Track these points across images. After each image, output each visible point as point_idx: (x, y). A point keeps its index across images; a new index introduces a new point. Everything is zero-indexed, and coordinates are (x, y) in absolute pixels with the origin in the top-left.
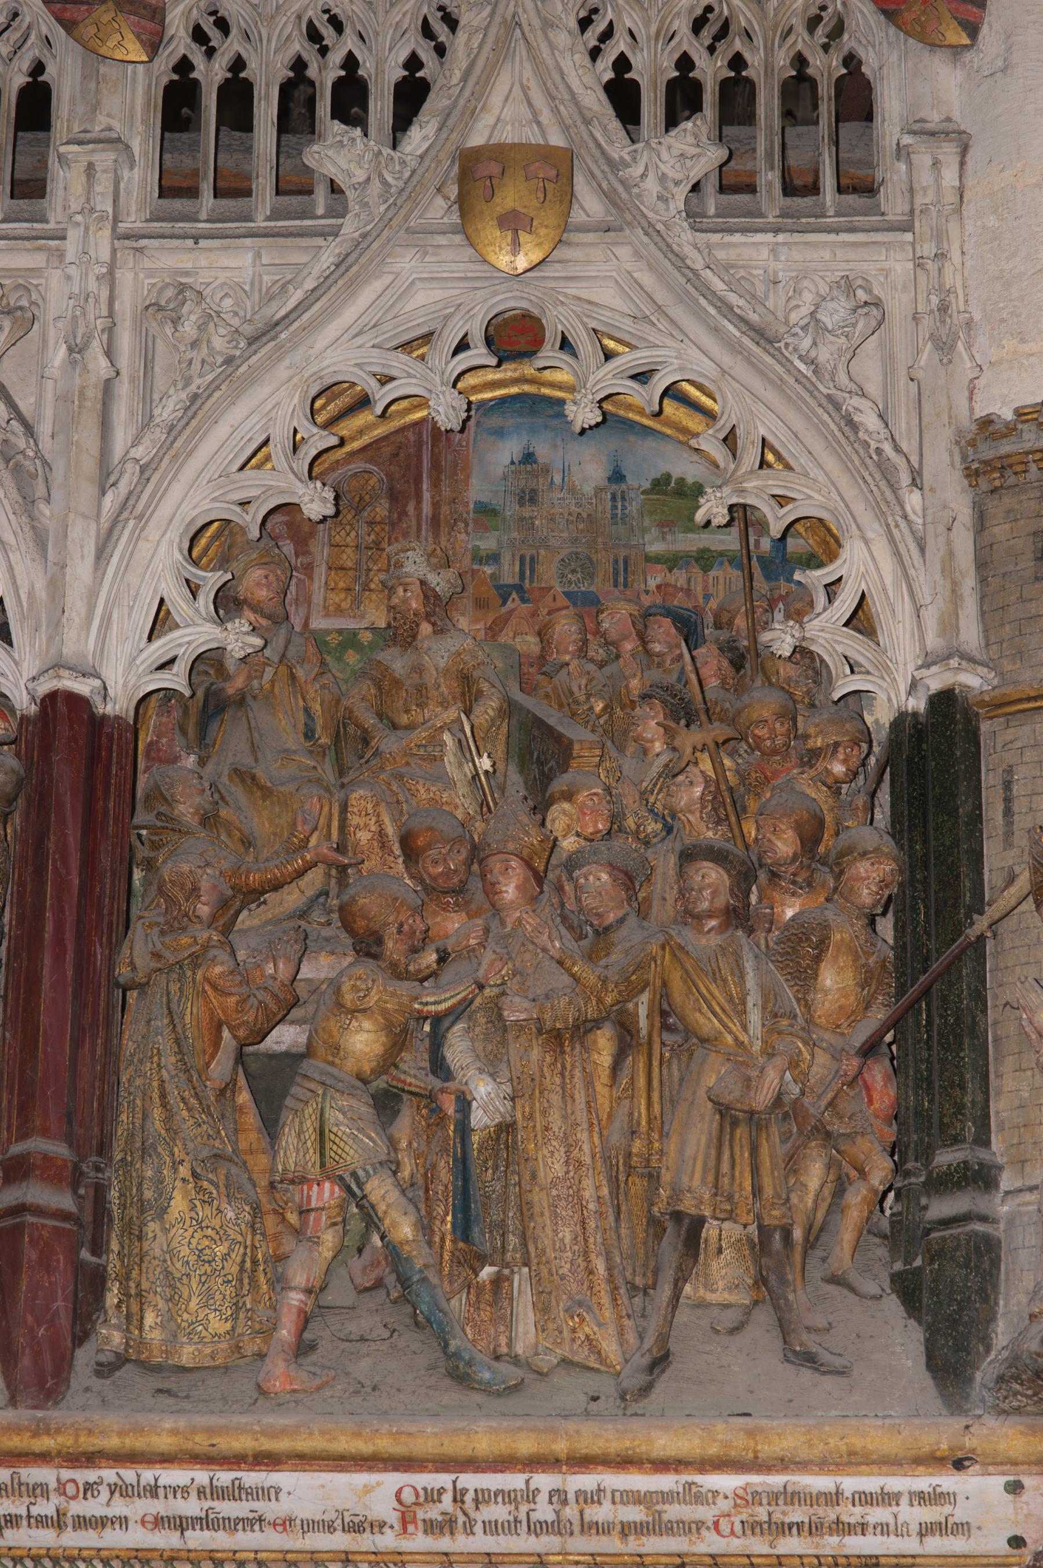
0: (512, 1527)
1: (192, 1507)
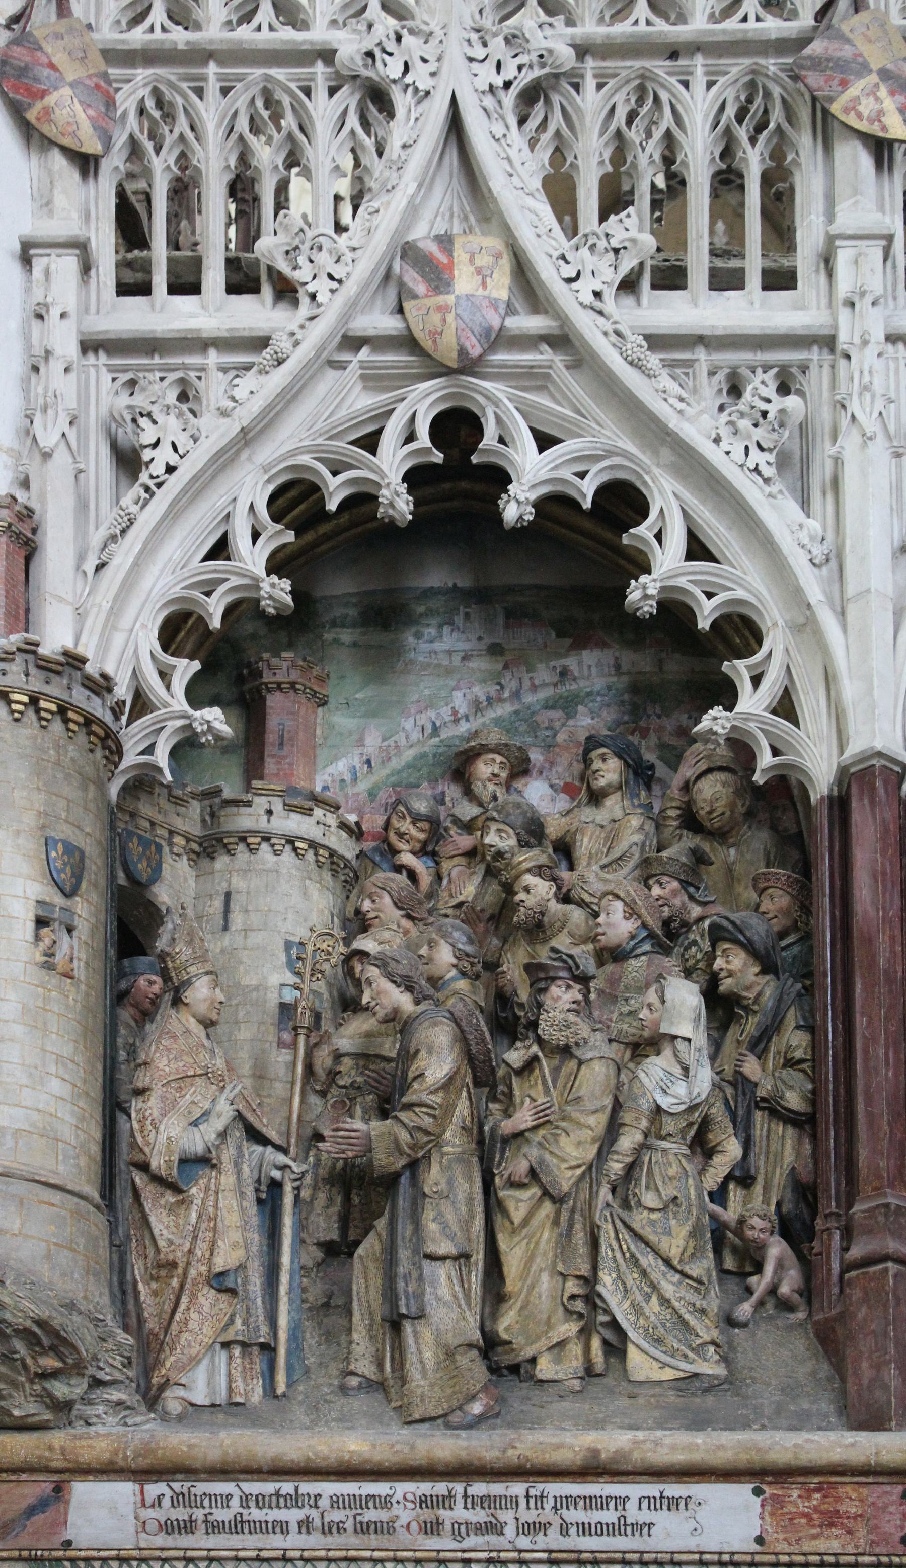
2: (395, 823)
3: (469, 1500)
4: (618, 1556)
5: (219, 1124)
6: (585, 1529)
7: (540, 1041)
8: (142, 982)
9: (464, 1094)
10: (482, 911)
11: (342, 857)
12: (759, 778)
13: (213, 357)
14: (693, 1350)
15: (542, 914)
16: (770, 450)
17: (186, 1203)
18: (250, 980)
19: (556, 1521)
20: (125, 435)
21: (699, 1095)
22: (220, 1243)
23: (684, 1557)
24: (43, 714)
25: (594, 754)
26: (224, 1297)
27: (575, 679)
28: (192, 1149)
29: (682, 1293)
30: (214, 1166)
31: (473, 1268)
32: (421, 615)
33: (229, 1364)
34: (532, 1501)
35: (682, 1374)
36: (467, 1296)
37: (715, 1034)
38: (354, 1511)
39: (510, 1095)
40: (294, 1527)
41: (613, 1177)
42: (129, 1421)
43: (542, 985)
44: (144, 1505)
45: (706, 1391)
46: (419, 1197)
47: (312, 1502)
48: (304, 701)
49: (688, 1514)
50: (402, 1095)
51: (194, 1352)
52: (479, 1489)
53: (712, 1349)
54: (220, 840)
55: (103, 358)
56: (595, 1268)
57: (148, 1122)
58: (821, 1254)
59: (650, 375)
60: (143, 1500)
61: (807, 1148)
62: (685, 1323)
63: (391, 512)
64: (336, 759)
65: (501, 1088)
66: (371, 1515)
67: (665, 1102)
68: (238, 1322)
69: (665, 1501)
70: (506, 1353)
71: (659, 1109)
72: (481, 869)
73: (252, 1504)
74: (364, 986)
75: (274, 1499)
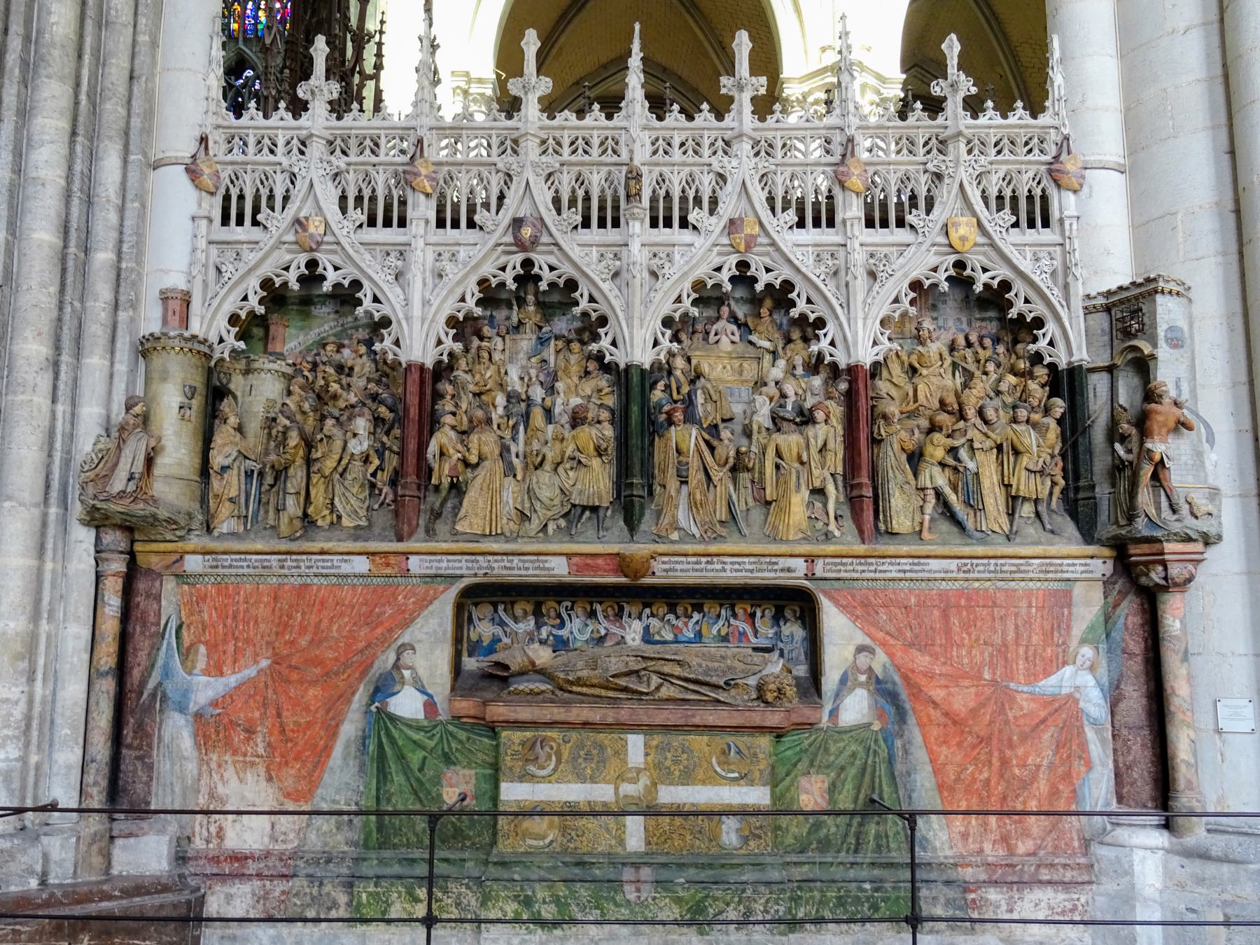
0: (984, 572)
1: (908, 568)
46: (286, 477)
52: (294, 557)
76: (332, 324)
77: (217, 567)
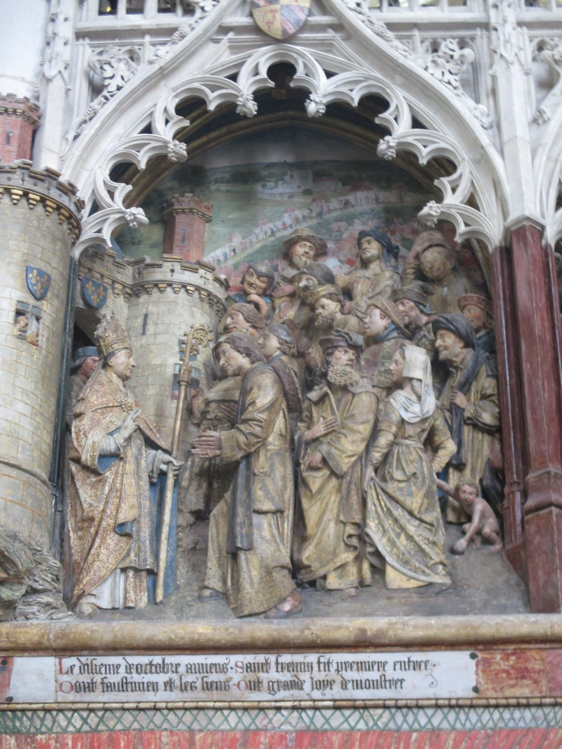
2: (248, 278)
3: (280, 666)
4: (381, 702)
5: (126, 433)
6: (358, 685)
7: (330, 385)
8: (89, 360)
9: (281, 414)
10: (298, 324)
11: (216, 297)
12: (458, 239)
13: (148, 39)
14: (428, 568)
15: (333, 320)
16: (456, 74)
17: (102, 481)
18: (157, 361)
19: (339, 680)
20: (97, 78)
21: (428, 412)
22: (122, 505)
23: (425, 703)
24: (31, 201)
25: (364, 240)
26: (124, 539)
27: (353, 206)
28: (108, 449)
29: (420, 531)
30: (121, 459)
31: (286, 520)
32: (266, 176)
33: (126, 582)
34: (322, 666)
35: (421, 584)
36: (281, 535)
37: (438, 385)
38: (202, 675)
39: (311, 418)
40: (161, 686)
41: (375, 462)
42: (54, 617)
43: (330, 351)
44: (61, 672)
45: (438, 593)
46: (251, 476)
47: (174, 669)
48: (198, 219)
49: (427, 672)
50: (242, 414)
51: (102, 574)
52: (286, 658)
53: (441, 567)
54: (143, 286)
55: (87, 41)
56: (364, 518)
57: (82, 433)
58: (509, 508)
59: (387, 40)
60: (61, 669)
61: (498, 446)
62: (422, 551)
63: (244, 110)
64: (216, 248)
65: (305, 413)
66: (214, 677)
67: (406, 416)
68: (132, 555)
69: (412, 664)
70: (307, 573)
71: (403, 421)
72: (298, 303)
73: (134, 671)
74: (221, 355)
75: (148, 667)
76: (299, 214)
77: (90, 687)
